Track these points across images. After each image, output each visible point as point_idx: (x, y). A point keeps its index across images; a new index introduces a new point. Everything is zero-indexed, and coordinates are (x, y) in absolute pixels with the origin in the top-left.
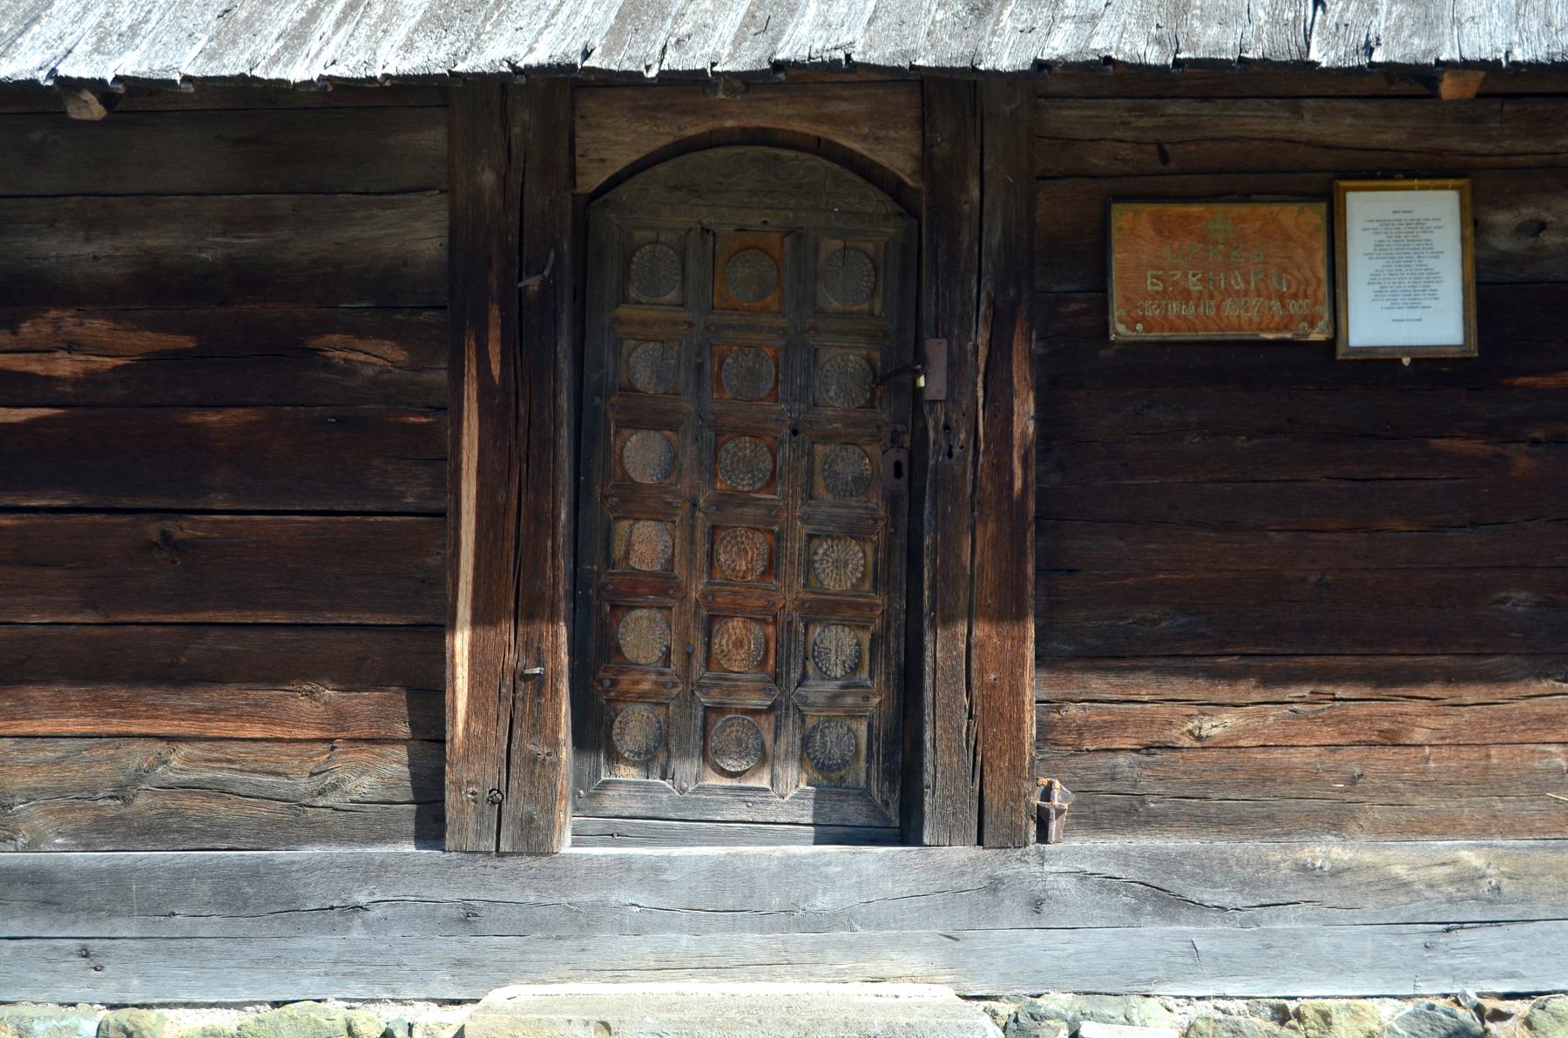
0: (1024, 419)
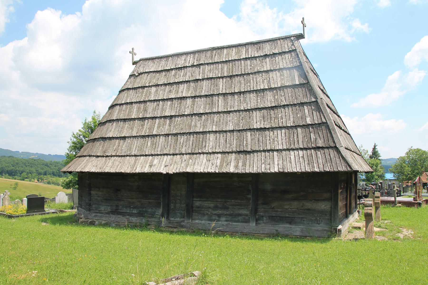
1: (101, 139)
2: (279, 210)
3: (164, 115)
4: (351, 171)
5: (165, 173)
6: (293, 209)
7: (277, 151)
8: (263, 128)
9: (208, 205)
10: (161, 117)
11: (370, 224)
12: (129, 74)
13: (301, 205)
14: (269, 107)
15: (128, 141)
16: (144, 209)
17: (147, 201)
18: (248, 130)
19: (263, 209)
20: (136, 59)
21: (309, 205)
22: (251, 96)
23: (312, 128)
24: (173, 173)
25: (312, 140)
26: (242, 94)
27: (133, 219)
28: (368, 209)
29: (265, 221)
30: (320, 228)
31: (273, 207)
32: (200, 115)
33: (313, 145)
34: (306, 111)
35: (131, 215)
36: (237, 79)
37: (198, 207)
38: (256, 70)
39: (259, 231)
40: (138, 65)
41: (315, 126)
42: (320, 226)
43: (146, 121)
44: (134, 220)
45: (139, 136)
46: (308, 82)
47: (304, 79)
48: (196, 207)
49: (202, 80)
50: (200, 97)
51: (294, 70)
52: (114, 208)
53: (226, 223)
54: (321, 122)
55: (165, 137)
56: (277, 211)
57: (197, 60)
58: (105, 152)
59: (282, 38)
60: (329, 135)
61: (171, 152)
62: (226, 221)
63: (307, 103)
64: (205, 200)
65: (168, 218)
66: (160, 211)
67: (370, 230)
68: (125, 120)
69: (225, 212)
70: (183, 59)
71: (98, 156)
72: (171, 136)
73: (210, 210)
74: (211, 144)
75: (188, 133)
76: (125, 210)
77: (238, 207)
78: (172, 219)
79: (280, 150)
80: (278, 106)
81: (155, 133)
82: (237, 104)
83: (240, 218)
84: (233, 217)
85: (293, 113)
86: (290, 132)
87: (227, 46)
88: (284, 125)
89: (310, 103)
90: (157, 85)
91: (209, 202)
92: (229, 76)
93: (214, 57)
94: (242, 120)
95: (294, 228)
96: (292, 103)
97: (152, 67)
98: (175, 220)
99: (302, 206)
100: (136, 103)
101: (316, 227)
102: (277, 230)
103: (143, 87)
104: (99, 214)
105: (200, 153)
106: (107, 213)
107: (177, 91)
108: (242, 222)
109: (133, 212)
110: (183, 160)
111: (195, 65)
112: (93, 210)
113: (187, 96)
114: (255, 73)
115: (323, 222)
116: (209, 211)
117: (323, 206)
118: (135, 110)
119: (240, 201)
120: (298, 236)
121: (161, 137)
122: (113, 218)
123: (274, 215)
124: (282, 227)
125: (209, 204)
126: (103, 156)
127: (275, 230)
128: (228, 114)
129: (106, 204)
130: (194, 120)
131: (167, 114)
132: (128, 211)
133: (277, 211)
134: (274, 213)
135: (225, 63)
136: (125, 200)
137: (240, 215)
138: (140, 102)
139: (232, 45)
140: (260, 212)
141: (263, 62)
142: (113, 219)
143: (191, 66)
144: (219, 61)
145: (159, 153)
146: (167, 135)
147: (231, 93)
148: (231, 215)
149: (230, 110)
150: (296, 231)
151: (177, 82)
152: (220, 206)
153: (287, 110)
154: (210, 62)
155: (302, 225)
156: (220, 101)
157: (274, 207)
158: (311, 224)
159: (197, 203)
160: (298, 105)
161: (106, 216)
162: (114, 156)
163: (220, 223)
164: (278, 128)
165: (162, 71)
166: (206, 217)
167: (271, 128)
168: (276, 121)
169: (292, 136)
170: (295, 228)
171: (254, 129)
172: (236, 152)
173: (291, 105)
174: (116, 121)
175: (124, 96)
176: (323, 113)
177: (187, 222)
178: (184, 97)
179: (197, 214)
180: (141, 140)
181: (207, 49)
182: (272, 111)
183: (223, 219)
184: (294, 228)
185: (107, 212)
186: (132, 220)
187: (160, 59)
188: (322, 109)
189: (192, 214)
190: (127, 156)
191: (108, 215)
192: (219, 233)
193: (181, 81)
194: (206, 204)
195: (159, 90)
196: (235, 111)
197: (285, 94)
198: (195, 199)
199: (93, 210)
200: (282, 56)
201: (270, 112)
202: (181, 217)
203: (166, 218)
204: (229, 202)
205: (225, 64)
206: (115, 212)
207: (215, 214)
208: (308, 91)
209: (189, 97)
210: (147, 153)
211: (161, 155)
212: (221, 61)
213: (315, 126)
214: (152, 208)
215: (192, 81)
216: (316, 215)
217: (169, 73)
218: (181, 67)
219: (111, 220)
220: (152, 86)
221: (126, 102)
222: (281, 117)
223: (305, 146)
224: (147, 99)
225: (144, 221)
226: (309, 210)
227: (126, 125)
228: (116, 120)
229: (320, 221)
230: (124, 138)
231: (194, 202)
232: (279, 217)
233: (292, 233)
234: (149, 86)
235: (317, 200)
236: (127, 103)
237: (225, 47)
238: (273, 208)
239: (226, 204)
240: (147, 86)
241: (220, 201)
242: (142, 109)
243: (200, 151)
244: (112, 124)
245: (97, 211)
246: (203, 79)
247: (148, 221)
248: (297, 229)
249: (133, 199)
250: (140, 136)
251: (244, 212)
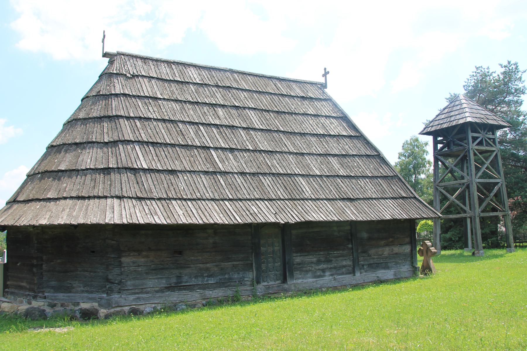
16: (227, 276)
17: (230, 263)
19: (362, 258)
21: (396, 249)
37: (300, 264)
48: (297, 264)
52: (174, 280)
56: (374, 259)
64: (306, 254)
69: (329, 266)
73: (313, 265)
76: (193, 281)
77: (341, 258)
84: (337, 270)
91: (311, 257)
102: (378, 277)
108: (346, 274)
122: (175, 297)
123: (372, 262)
124: (382, 274)
129: (156, 277)
132: (200, 283)
133: (374, 259)
136: (192, 266)
137: (344, 267)
148: (335, 268)
152: (323, 259)
158: (399, 266)
159: (298, 259)
166: (310, 274)
185: (157, 289)
202: (277, 279)
204: (331, 254)
206: (178, 287)
207: (319, 270)
214: (239, 273)
219: (171, 301)
225: (229, 293)
226: (396, 254)
232: (376, 263)
239: (328, 256)
248: (389, 274)
249: (206, 263)
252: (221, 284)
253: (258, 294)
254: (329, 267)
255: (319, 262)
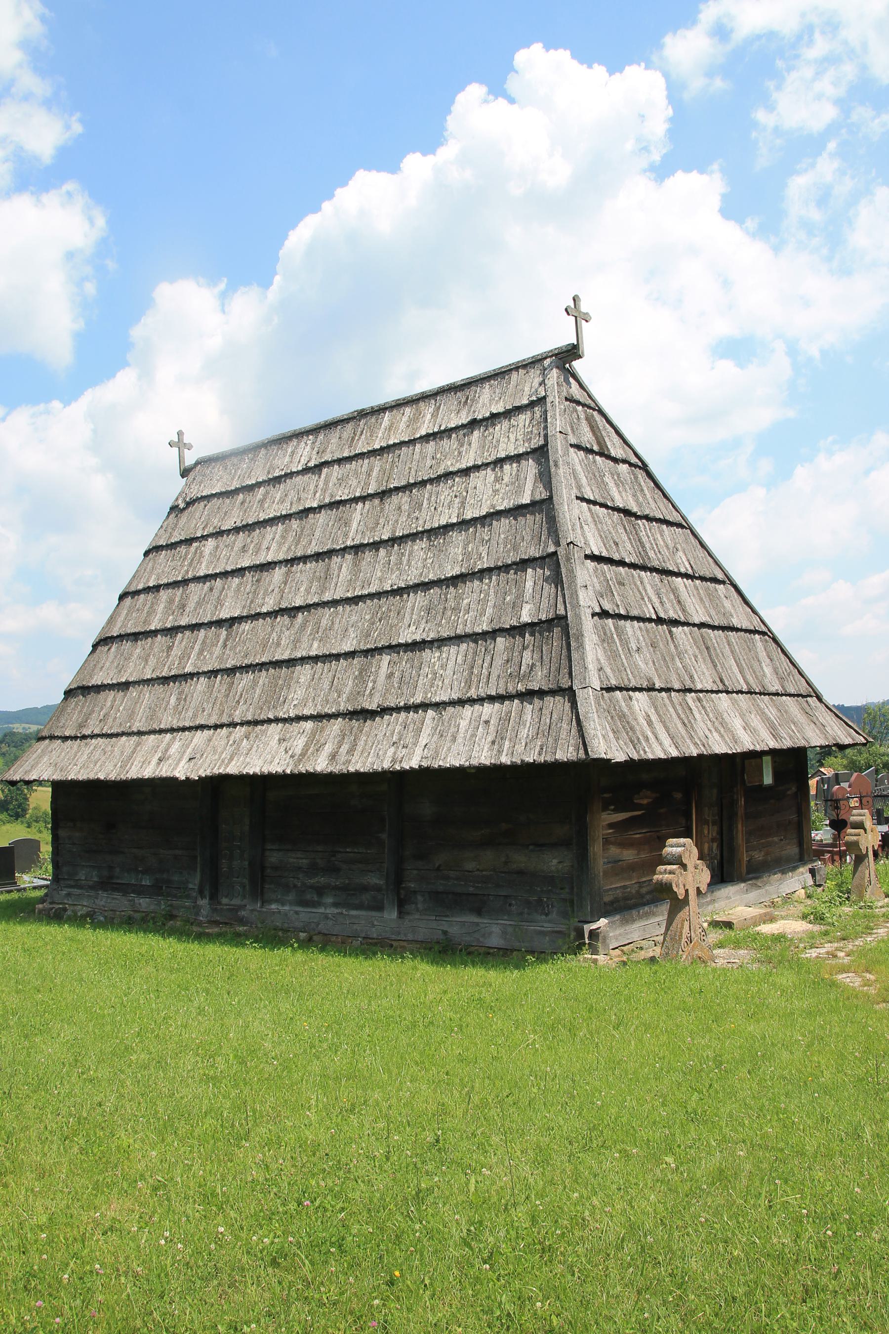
0: (743, 803)
1: (79, 691)
2: (452, 874)
3: (217, 619)
4: (586, 759)
5: (183, 778)
6: (484, 873)
7: (435, 708)
8: (420, 643)
9: (295, 860)
10: (210, 624)
11: (678, 916)
12: (170, 505)
13: (503, 859)
14: (447, 579)
15: (133, 692)
16: (165, 876)
18: (386, 650)
19: (415, 872)
20: (190, 459)
21: (521, 859)
22: (416, 547)
23: (532, 634)
24: (197, 778)
25: (522, 672)
26: (396, 545)
27: (141, 901)
28: (666, 870)
29: (420, 906)
30: (548, 927)
31: (437, 865)
32: (292, 611)
33: (519, 685)
34: (529, 584)
35: (140, 891)
36: (395, 499)
38: (441, 471)
39: (405, 935)
40: (192, 475)
41: (541, 627)
42: (549, 922)
43: (180, 635)
44: (144, 903)
45: (156, 679)
46: (551, 498)
47: (544, 487)
49: (317, 510)
50: (304, 559)
51: (530, 460)
53: (336, 911)
54: (554, 616)
55: (209, 678)
57: (318, 453)
58: (81, 726)
59: (524, 363)
60: (564, 652)
61: (212, 721)
62: (336, 905)
63: (535, 559)
65: (214, 897)
66: (194, 882)
67: (675, 934)
68: (135, 636)
69: (334, 881)
70: (290, 450)
71: (65, 738)
72: (222, 676)
73: (301, 876)
74: (299, 692)
75: (257, 664)
78: (225, 901)
79: (442, 703)
80: (468, 574)
81: (188, 669)
82: (379, 574)
83: (366, 897)
85: (496, 593)
86: (479, 649)
87: (393, 404)
88: (468, 630)
89: (542, 558)
90: (219, 534)
92: (379, 493)
93: (358, 440)
94: (380, 620)
95: (484, 926)
96: (500, 564)
97: (218, 481)
98: (233, 902)
99: (506, 863)
100: (168, 585)
101: (541, 924)
102: (445, 933)
103: (189, 541)
104: (76, 890)
105: (269, 721)
106: (92, 888)
107: (258, 546)
109: (144, 883)
110: (231, 742)
111: (310, 468)
112: (64, 879)
113: (275, 560)
114: (439, 478)
115: (555, 910)
116: (298, 879)
117: (555, 862)
118: (162, 606)
119: (364, 851)
120: (495, 948)
121: (202, 679)
122: (103, 900)
123: (441, 888)
125: (297, 858)
126: (75, 738)
127: (441, 932)
128: (353, 606)
129: (88, 864)
130: (278, 629)
131: (225, 614)
132: (133, 882)
134: (442, 882)
135: (379, 455)
137: (365, 888)
138: (175, 584)
139: (404, 399)
140: (409, 881)
141: (462, 446)
142: (102, 903)
143: (301, 471)
144: (365, 451)
145: (187, 725)
146: (213, 673)
147: (372, 544)
148: (344, 889)
149: (360, 594)
150: (491, 933)
151: (262, 519)
153: (486, 584)
154: (346, 454)
155: (506, 918)
156: (344, 569)
157: (440, 866)
158: (529, 914)
159: (273, 858)
160: (514, 567)
161: (89, 896)
162: (98, 736)
163: (322, 910)
164: (453, 641)
165: (236, 491)
166: (291, 897)
167: (437, 640)
168: (453, 618)
169: (480, 662)
170: (487, 925)
171: (399, 645)
172: (346, 714)
173: (498, 568)
174: (119, 639)
175: (145, 570)
176: (563, 589)
177: (250, 909)
178: (269, 563)
179: (272, 886)
180: (159, 689)
181: (346, 417)
182: (452, 589)
183: (329, 900)
184: (484, 926)
186: (140, 904)
187: (239, 457)
188: (564, 576)
189: (263, 888)
190: (123, 734)
191: (92, 893)
192: (315, 938)
193: (271, 516)
194: (292, 860)
195: (221, 546)
196: (371, 596)
197: (493, 534)
198: (269, 846)
199: (64, 879)
200: (512, 420)
201: (446, 595)
203: (211, 899)
204: (340, 852)
205: (378, 457)
206: (107, 884)
207: (312, 887)
208: (547, 523)
209: (280, 562)
210: (162, 726)
211: (190, 729)
212: (370, 449)
213: (541, 627)
215: (296, 516)
216: (539, 889)
217: (251, 494)
218: (280, 477)
220: (208, 536)
221: (147, 586)
222: (467, 608)
223: (502, 691)
224: (190, 576)
226: (520, 872)
227: (138, 651)
228: (118, 637)
229: (548, 906)
230: (125, 686)
231: (267, 853)
233: (481, 939)
234: (202, 537)
235: (540, 846)
236: (149, 588)
237: (387, 406)
238: (438, 869)
239: (333, 859)
240: (197, 538)
241: (320, 850)
242: (176, 603)
243: (271, 716)
244: (109, 649)
245: (71, 883)
246: (320, 507)
247: (171, 905)
250: (158, 678)
251: (374, 880)
252: (156, 890)
253: (201, 918)
254: (333, 884)
255: (313, 869)
